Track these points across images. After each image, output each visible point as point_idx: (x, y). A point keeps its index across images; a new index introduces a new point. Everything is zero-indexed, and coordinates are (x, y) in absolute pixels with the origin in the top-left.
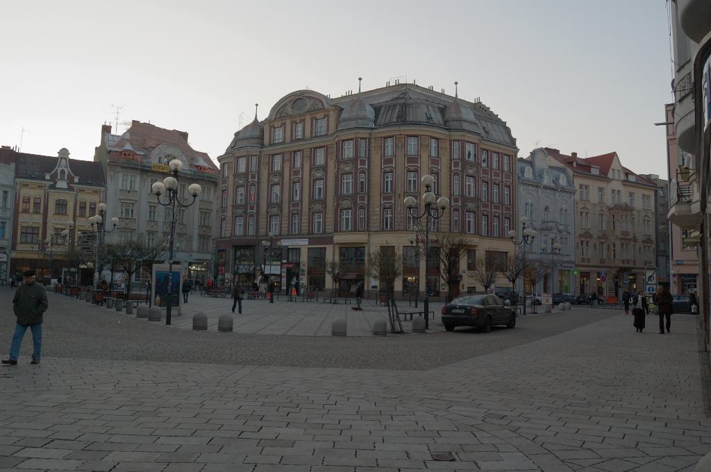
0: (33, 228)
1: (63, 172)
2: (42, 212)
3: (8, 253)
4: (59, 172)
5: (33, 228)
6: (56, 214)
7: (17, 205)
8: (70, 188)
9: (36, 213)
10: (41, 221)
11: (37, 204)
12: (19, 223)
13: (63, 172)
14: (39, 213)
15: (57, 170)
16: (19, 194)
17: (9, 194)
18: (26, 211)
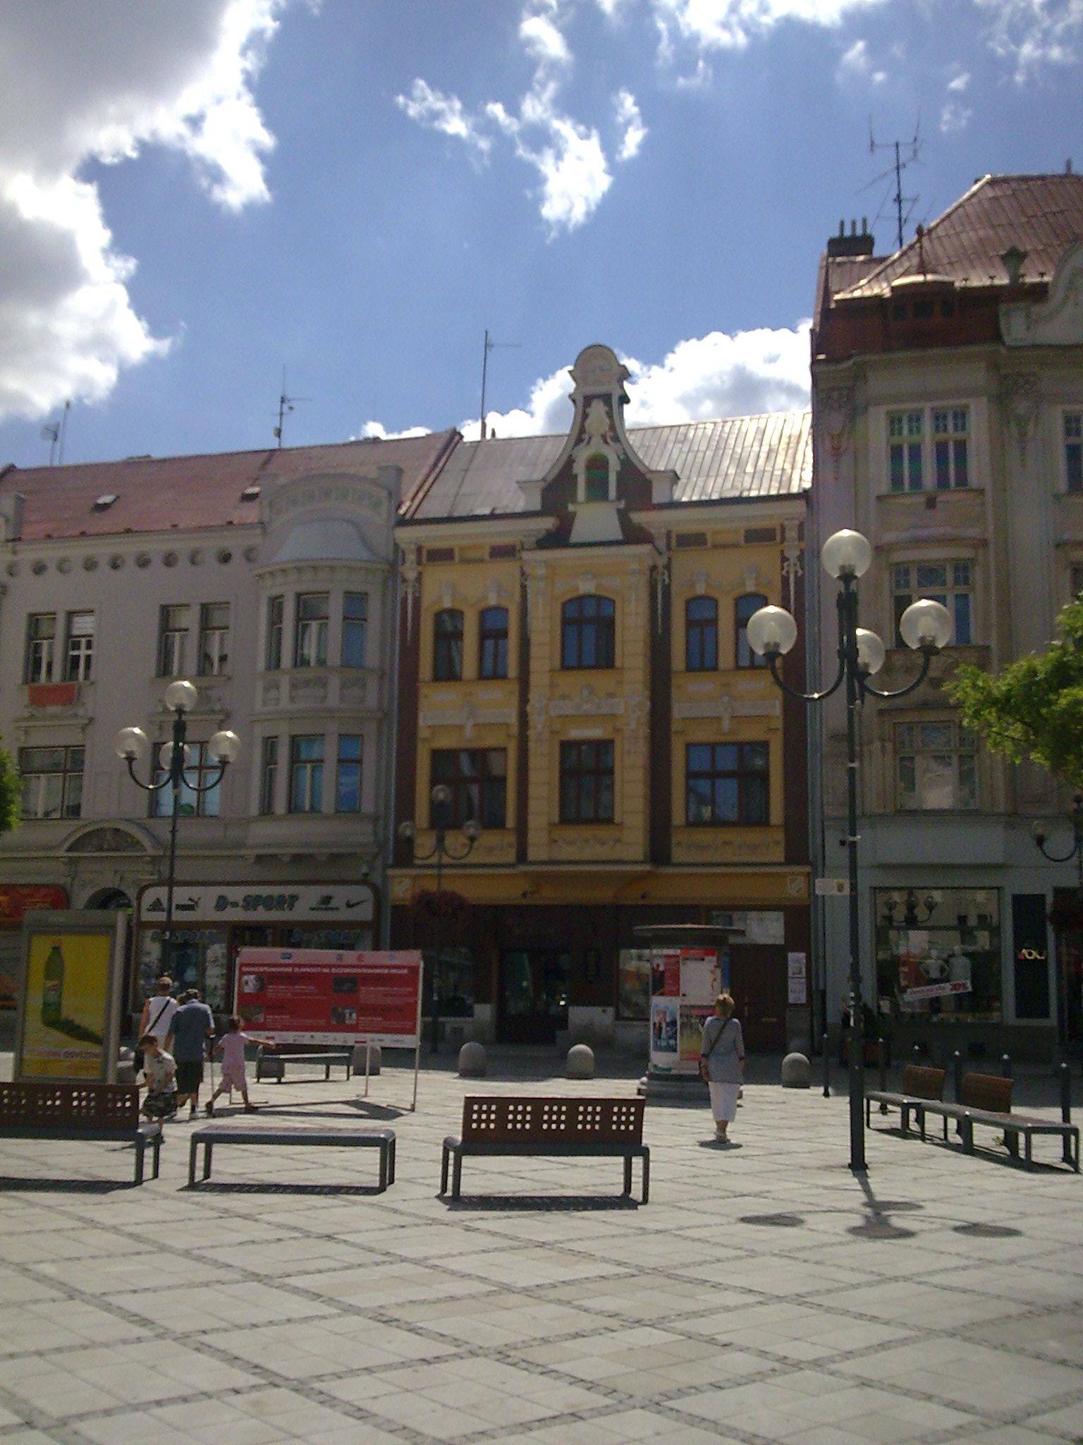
0: (479, 756)
1: (597, 465)
2: (513, 670)
3: (376, 878)
4: (579, 469)
5: (740, 746)
6: (565, 667)
7: (410, 653)
8: (633, 535)
9: (491, 673)
10: (513, 719)
11: (492, 632)
12: (423, 733)
13: (597, 465)
14: (504, 677)
15: (570, 462)
16: (417, 602)
17: (374, 609)
18: (447, 672)
